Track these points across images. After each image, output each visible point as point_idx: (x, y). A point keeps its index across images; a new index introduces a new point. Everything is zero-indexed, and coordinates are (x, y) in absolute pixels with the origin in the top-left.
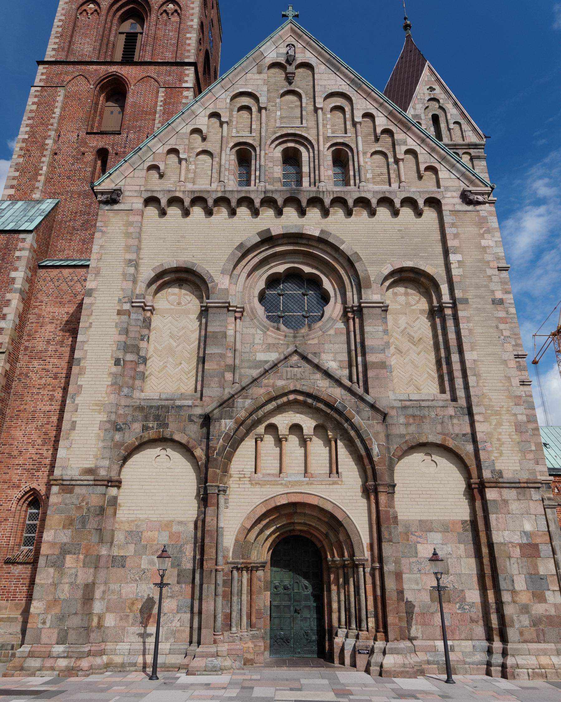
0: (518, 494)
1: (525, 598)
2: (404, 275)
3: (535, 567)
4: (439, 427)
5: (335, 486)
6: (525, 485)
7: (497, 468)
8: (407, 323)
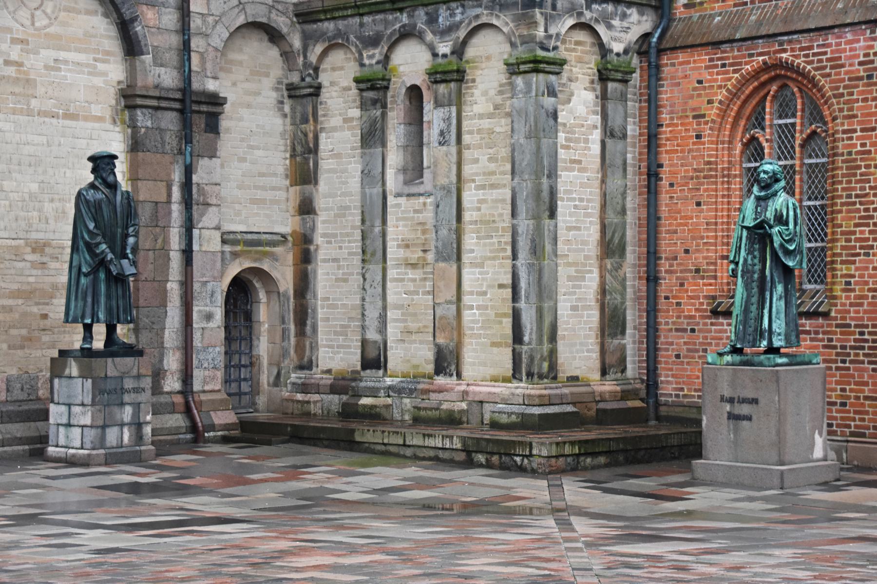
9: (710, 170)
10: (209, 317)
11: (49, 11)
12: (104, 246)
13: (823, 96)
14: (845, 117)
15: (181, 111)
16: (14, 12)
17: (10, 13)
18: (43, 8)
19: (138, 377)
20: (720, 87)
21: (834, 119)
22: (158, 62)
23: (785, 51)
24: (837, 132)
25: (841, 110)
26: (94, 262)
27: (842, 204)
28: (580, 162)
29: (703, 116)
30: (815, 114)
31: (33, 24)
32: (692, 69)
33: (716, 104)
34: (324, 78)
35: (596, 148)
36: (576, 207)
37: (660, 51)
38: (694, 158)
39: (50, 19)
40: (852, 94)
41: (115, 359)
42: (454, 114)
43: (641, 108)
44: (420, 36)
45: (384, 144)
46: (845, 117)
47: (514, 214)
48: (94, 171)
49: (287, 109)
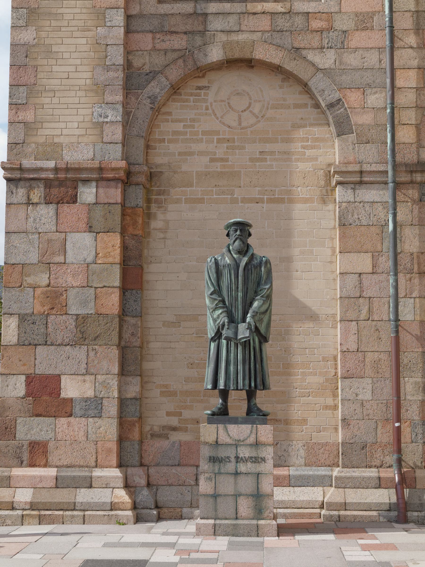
11: (256, 111)
16: (222, 117)
17: (217, 118)
18: (251, 109)
26: (216, 327)
31: (240, 124)
39: (257, 117)
41: (227, 425)
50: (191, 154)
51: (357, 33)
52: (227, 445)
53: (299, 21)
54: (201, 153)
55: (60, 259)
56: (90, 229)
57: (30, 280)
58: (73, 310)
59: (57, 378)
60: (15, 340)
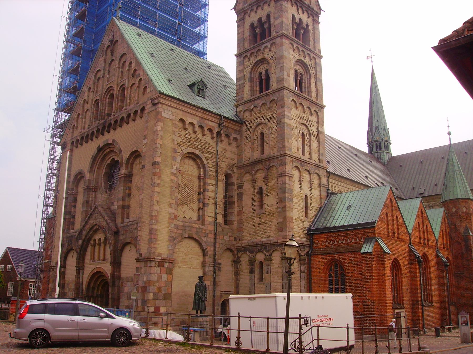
0: (145, 264)
1: (140, 309)
2: (137, 154)
3: (144, 296)
4: (131, 234)
5: (107, 264)
6: (146, 260)
7: (141, 253)
8: (138, 180)
9: (322, 279)
10: (218, 309)
12: (201, 295)
13: (343, 265)
14: (348, 270)
15: (214, 267)
19: (207, 322)
20: (323, 263)
21: (346, 270)
22: (210, 257)
23: (336, 256)
24: (346, 272)
25: (347, 268)
27: (348, 287)
28: (296, 278)
29: (320, 268)
30: (342, 268)
32: (317, 259)
33: (323, 266)
34: (241, 259)
35: (299, 275)
36: (295, 287)
37: (311, 255)
38: (319, 277)
40: (349, 265)
42: (270, 267)
43: (307, 266)
44: (262, 252)
45: (254, 273)
46: (348, 270)
47: (283, 289)
48: (199, 279)
49: (233, 266)
50: (179, 256)
51: (210, 234)
52: (203, 322)
53: (201, 230)
54: (181, 256)
55: (161, 280)
56: (167, 274)
57: (155, 285)
58: (163, 292)
59: (159, 308)
60: (152, 298)
